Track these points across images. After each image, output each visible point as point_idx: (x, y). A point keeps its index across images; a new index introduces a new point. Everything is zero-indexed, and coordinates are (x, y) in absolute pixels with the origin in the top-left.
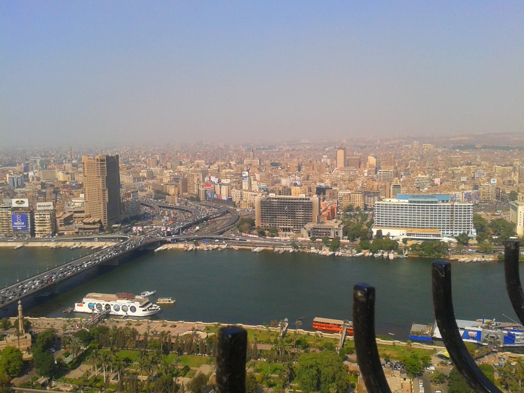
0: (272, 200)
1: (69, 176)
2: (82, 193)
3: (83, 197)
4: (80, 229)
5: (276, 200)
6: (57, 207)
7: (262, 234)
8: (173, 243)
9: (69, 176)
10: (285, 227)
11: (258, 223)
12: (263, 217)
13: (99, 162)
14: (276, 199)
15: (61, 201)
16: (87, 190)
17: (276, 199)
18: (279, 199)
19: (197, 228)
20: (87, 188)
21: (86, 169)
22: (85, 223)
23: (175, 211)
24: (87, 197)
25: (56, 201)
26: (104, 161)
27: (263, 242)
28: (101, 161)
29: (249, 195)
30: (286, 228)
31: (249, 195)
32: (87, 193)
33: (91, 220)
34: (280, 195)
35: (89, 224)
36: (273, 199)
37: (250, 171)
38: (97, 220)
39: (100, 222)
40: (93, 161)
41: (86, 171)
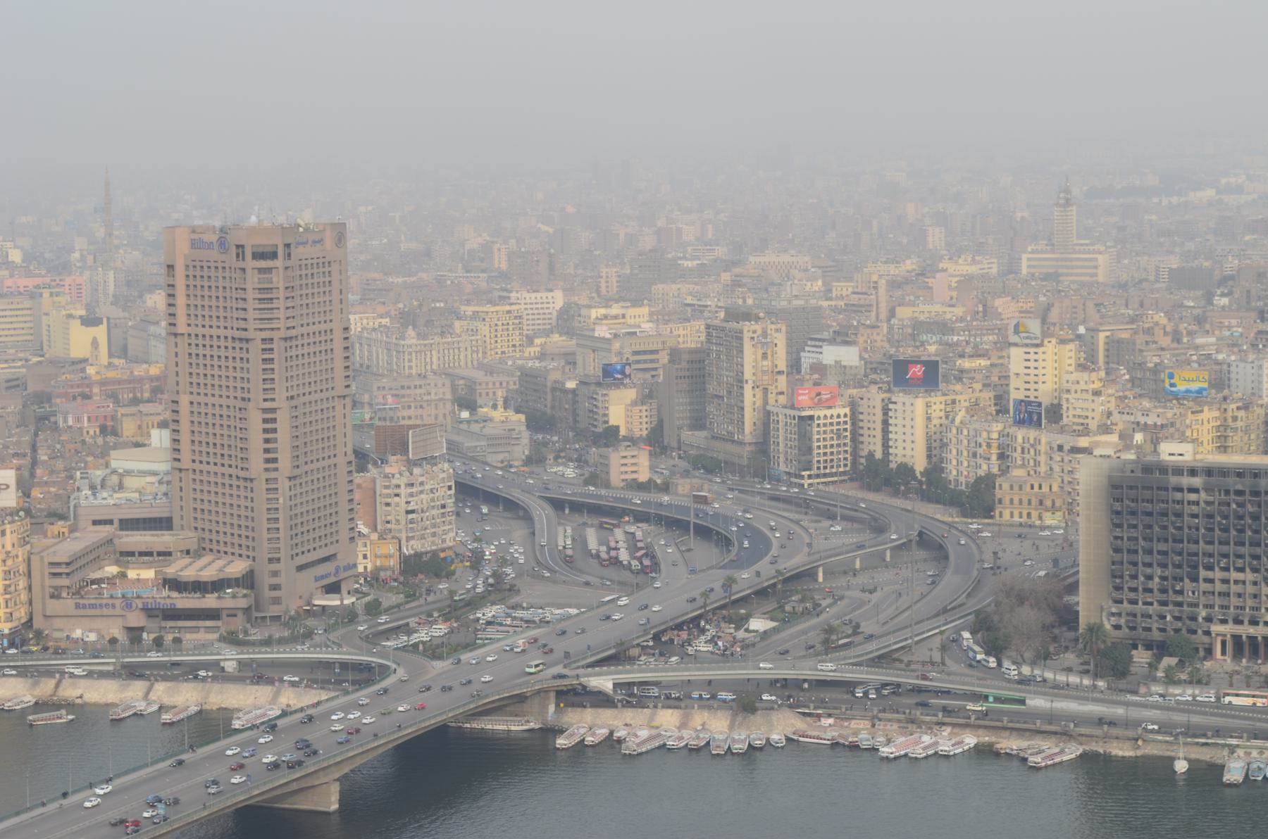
0: (1173, 480)
1: (100, 332)
2: (164, 425)
3: (167, 443)
4: (150, 612)
5: (1197, 481)
6: (36, 493)
7: (1111, 664)
8: (628, 705)
9: (100, 332)
10: (1246, 630)
11: (1090, 604)
12: (1121, 573)
13: (250, 263)
14: (1193, 472)
15: (60, 464)
16: (184, 407)
17: (1193, 472)
18: (1209, 472)
19: (758, 624)
20: (184, 400)
21: (181, 300)
22: (176, 585)
23: (639, 530)
24: (185, 446)
25: (34, 463)
26: (274, 255)
27: (1120, 711)
28: (256, 256)
29: (1043, 448)
30: (1252, 639)
31: (1043, 448)
32: (185, 426)
33: (207, 569)
34: (1223, 449)
35: (199, 587)
36: (1178, 471)
37: (1054, 315)
38: (237, 568)
39: (248, 581)
40: (214, 255)
41: (181, 311)
